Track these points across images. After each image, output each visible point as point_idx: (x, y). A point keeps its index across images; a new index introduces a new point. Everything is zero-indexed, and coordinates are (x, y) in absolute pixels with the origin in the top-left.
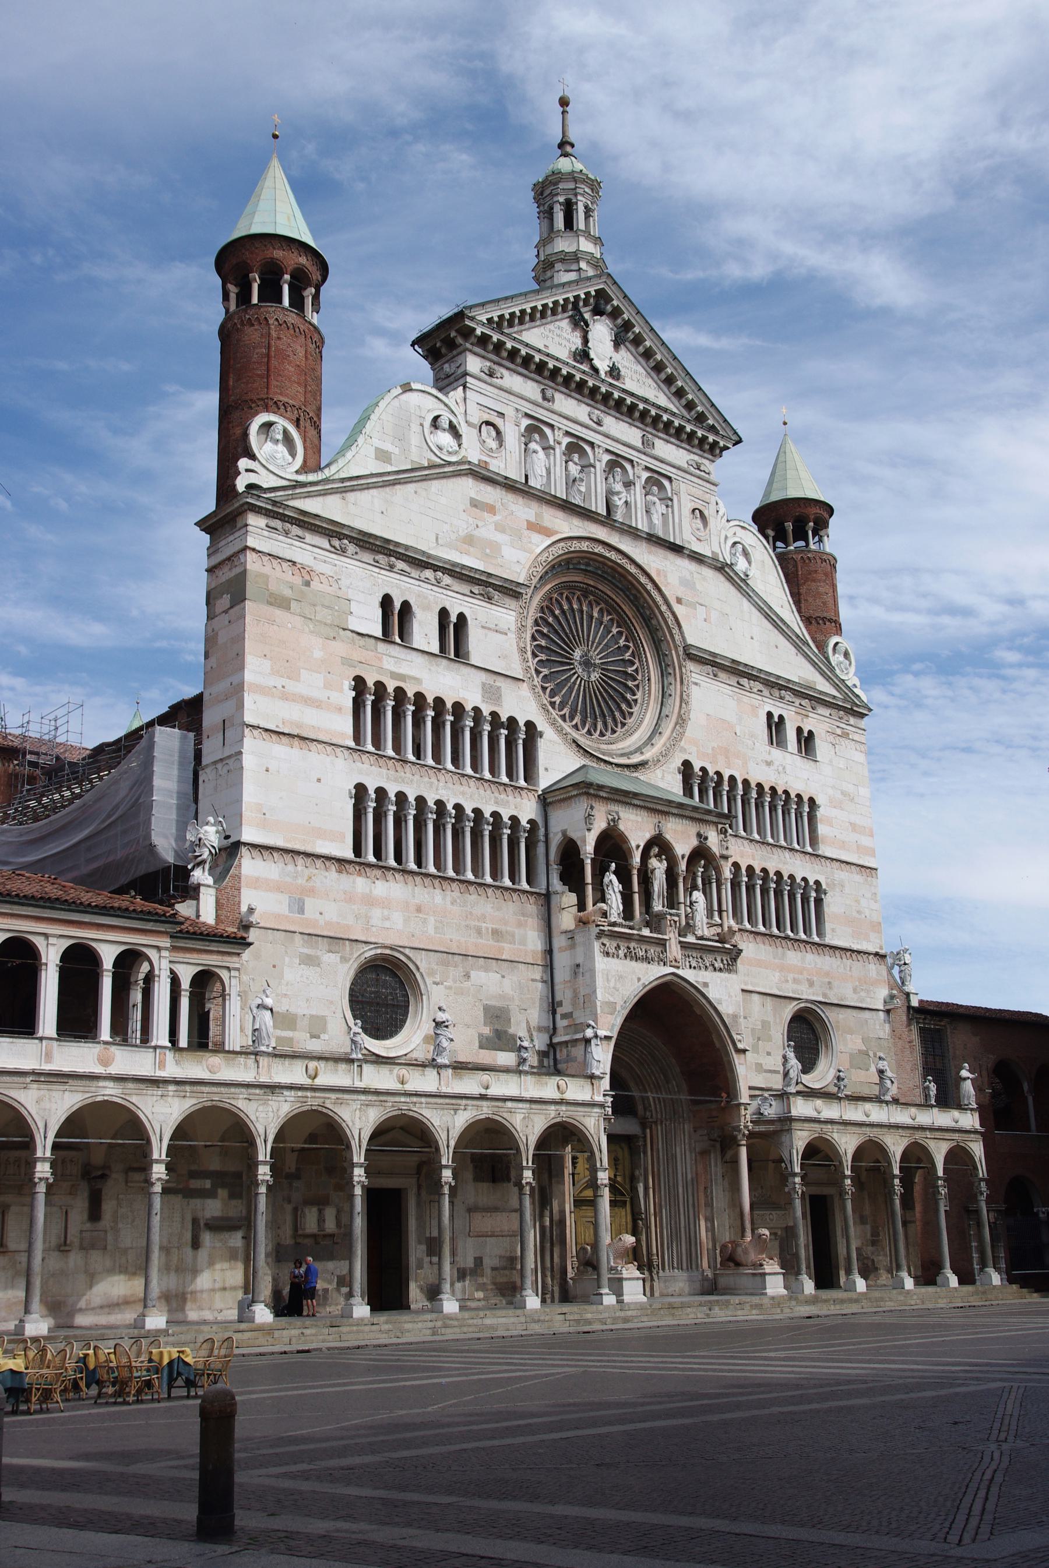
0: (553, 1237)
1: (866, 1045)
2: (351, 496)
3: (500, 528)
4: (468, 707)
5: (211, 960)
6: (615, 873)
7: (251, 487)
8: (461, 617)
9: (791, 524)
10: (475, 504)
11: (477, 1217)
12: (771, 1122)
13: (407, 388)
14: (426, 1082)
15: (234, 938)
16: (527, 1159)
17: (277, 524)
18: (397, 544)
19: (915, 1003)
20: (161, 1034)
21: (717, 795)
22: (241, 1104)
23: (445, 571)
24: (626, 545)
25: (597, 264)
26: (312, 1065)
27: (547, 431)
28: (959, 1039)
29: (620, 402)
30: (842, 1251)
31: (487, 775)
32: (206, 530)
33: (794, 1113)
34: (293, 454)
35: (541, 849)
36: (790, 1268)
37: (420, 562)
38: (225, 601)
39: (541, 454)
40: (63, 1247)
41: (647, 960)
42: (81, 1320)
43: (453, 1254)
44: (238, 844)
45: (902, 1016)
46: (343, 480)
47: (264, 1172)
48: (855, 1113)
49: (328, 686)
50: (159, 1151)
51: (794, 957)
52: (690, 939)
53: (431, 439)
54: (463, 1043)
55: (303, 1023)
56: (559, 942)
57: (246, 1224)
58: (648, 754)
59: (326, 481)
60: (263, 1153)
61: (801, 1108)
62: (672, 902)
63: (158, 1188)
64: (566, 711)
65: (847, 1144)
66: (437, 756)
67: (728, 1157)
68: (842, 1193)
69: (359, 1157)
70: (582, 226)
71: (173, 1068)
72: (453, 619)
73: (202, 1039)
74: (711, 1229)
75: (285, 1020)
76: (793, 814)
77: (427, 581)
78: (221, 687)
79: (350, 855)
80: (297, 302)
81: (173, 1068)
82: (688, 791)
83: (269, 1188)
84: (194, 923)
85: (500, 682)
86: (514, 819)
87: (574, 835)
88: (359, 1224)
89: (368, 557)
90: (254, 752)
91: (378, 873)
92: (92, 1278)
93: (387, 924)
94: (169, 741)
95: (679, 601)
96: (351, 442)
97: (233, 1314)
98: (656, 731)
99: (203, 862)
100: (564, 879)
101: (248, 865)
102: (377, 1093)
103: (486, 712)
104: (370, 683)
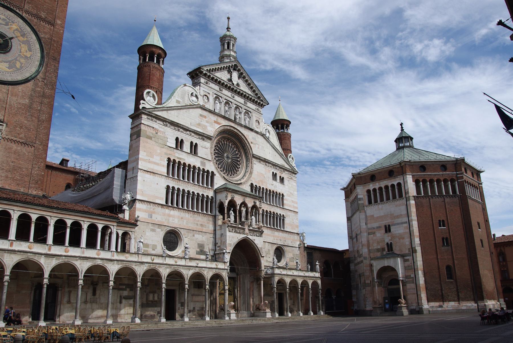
0: (213, 303)
1: (294, 256)
2: (169, 112)
3: (207, 122)
4: (197, 167)
5: (127, 229)
7: (143, 108)
8: (196, 144)
9: (280, 125)
10: (201, 115)
11: (194, 297)
12: (269, 275)
13: (185, 85)
14: (182, 262)
15: (133, 223)
16: (207, 283)
17: (150, 117)
18: (181, 124)
19: (306, 246)
20: (113, 248)
21: (259, 192)
22: (134, 267)
23: (192, 132)
24: (239, 128)
25: (235, 58)
26: (153, 257)
27: (220, 98)
28: (316, 255)
29: (239, 92)
30: (285, 307)
31: (201, 185)
32: (131, 118)
33: (275, 272)
34: (155, 100)
35: (214, 204)
36: (273, 311)
38: (135, 136)
39: (219, 104)
40: (86, 302)
41: (240, 233)
42: (90, 321)
43: (188, 306)
44: (135, 199)
45: (303, 249)
46: (167, 107)
47: (139, 284)
48: (290, 273)
49: (161, 160)
50: (112, 278)
51: (277, 233)
52: (251, 228)
53: (191, 98)
54: (192, 252)
55: (151, 246)
56: (218, 228)
57: (134, 297)
58: (242, 181)
59: (163, 107)
60: (139, 279)
61: (277, 271)
62: (247, 219)
63: (111, 288)
64: (222, 169)
65: (288, 280)
66: (188, 179)
67: (258, 283)
68: (286, 292)
69: (164, 281)
70: (231, 48)
71: (116, 257)
72: (194, 144)
73: (124, 249)
74: (253, 301)
75: (146, 245)
76: (278, 198)
77: (188, 134)
78: (133, 158)
79: (165, 203)
80: (158, 62)
81: (116, 257)
82: (252, 191)
83: (140, 288)
84: (123, 219)
85: (205, 161)
86: (207, 196)
87: (222, 201)
88: (163, 298)
89: (173, 127)
90: (141, 176)
91: (172, 208)
92: (93, 310)
93: (174, 222)
94: (118, 172)
95: (252, 143)
96: (170, 98)
97: (130, 320)
98: (244, 175)
99: (126, 204)
100: (220, 212)
101: (138, 205)
102: (169, 265)
103: (201, 169)
104: (172, 160)
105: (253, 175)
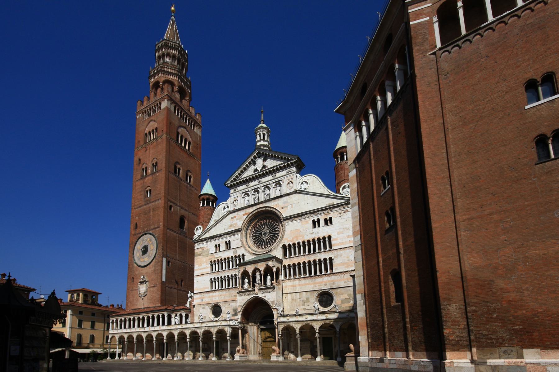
3: (237, 219)
10: (232, 218)
37: (220, 236)
51: (318, 280)
85: (237, 249)
95: (282, 208)
105: (285, 237)
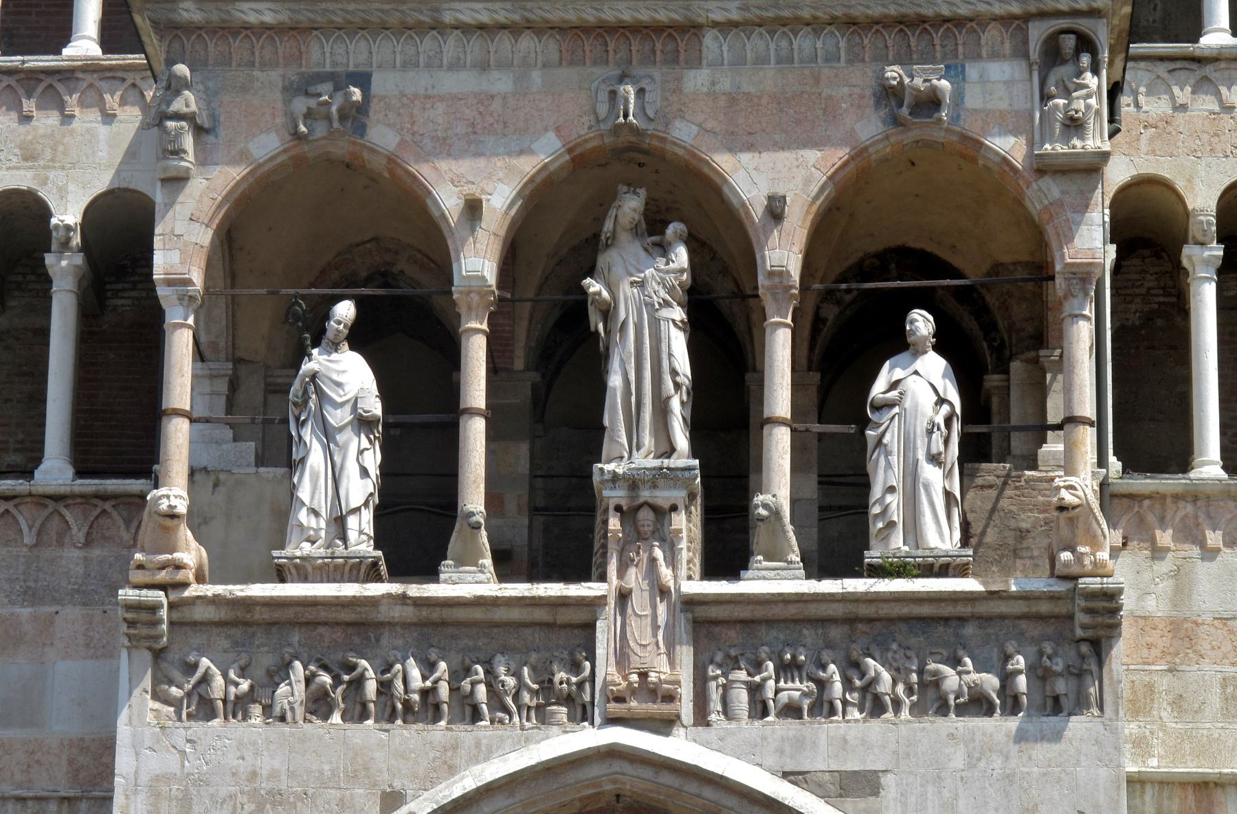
6: (359, 338)
52: (774, 579)
